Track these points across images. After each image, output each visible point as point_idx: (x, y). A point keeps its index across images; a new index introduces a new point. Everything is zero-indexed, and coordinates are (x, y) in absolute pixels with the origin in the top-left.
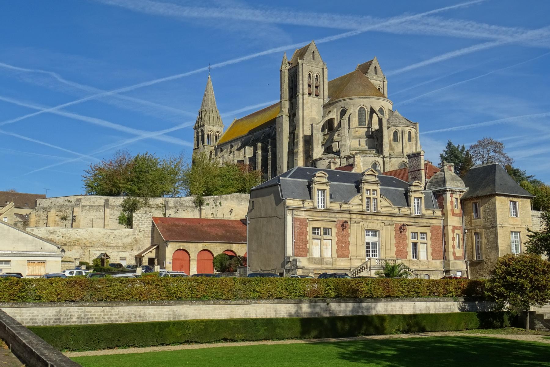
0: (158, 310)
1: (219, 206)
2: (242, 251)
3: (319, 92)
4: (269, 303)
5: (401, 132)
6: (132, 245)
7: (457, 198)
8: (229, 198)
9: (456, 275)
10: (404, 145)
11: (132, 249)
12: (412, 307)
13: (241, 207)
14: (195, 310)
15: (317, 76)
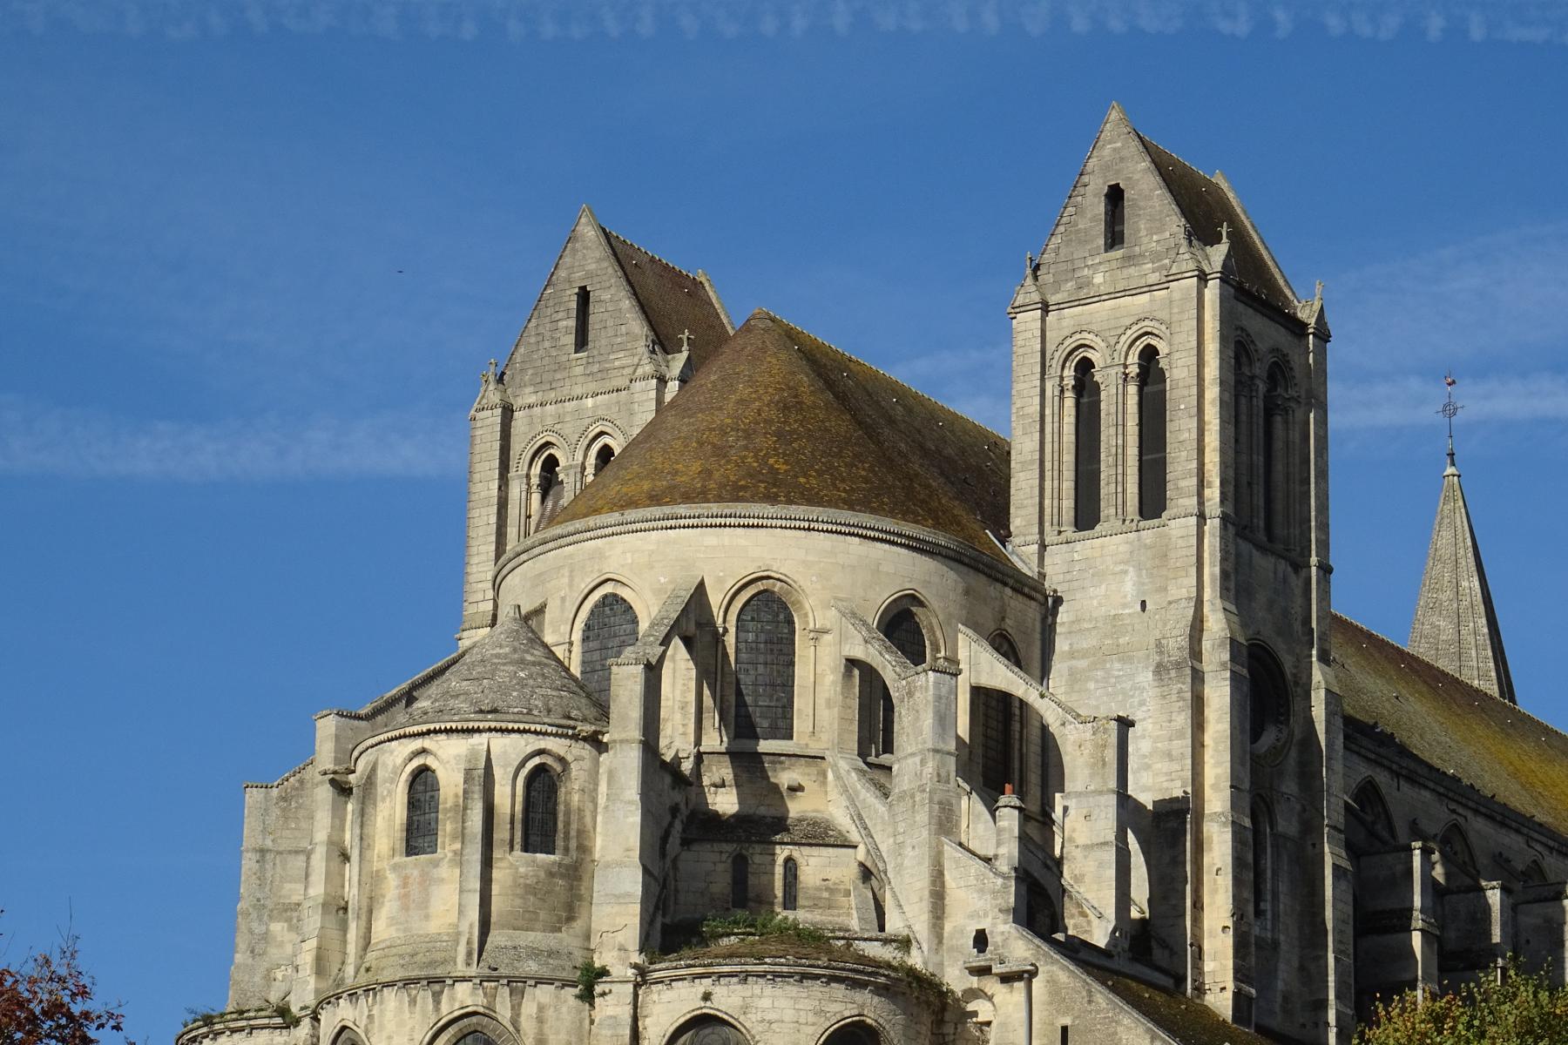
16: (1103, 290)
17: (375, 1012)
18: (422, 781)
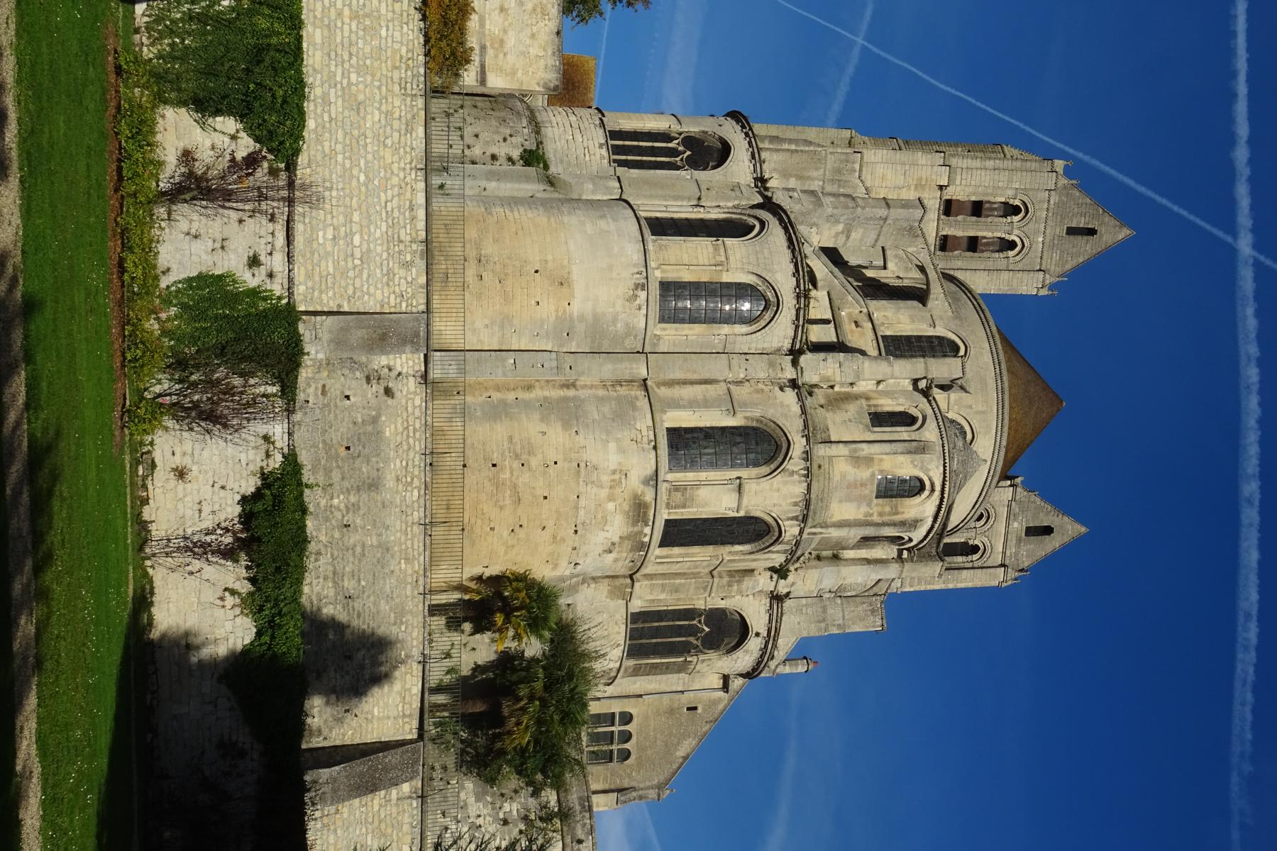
3: (956, 252)
5: (914, 436)
10: (866, 450)
15: (1012, 245)
16: (1010, 527)
17: (796, 477)
18: (915, 488)
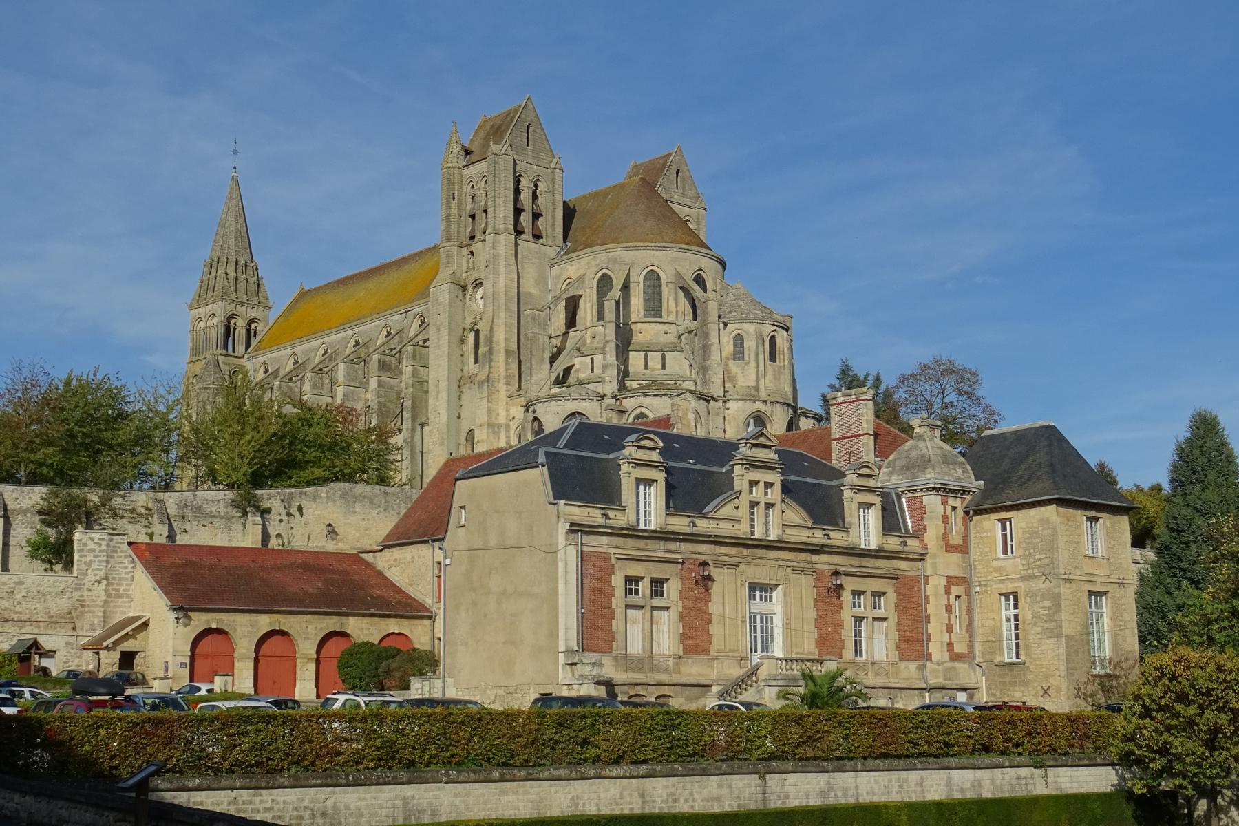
0: (368, 796)
1: (297, 514)
2: (372, 635)
4: (628, 774)
6: (72, 618)
7: (954, 508)
8: (323, 495)
9: (955, 699)
11: (74, 629)
12: (943, 783)
13: (353, 519)
14: (456, 796)
